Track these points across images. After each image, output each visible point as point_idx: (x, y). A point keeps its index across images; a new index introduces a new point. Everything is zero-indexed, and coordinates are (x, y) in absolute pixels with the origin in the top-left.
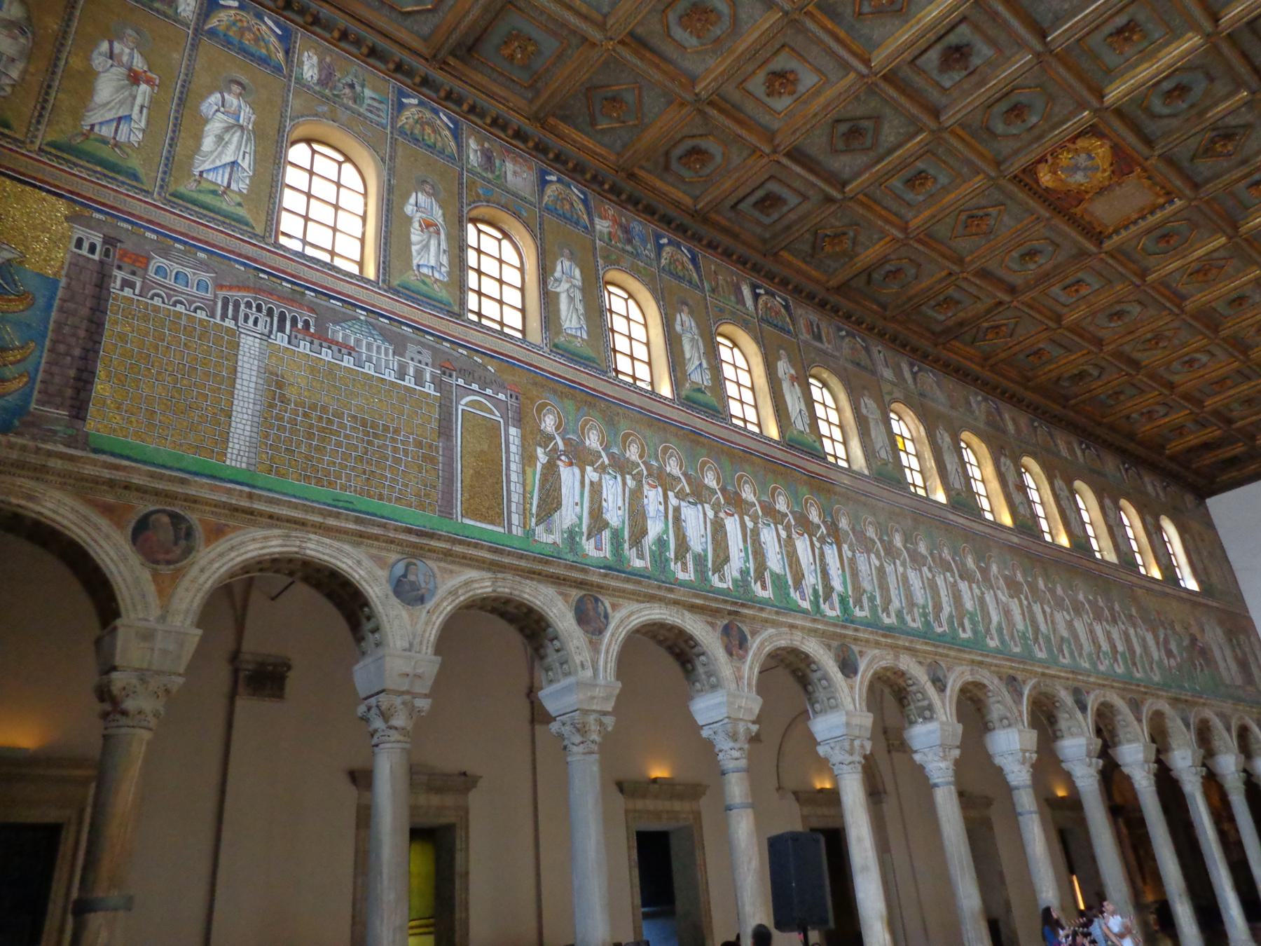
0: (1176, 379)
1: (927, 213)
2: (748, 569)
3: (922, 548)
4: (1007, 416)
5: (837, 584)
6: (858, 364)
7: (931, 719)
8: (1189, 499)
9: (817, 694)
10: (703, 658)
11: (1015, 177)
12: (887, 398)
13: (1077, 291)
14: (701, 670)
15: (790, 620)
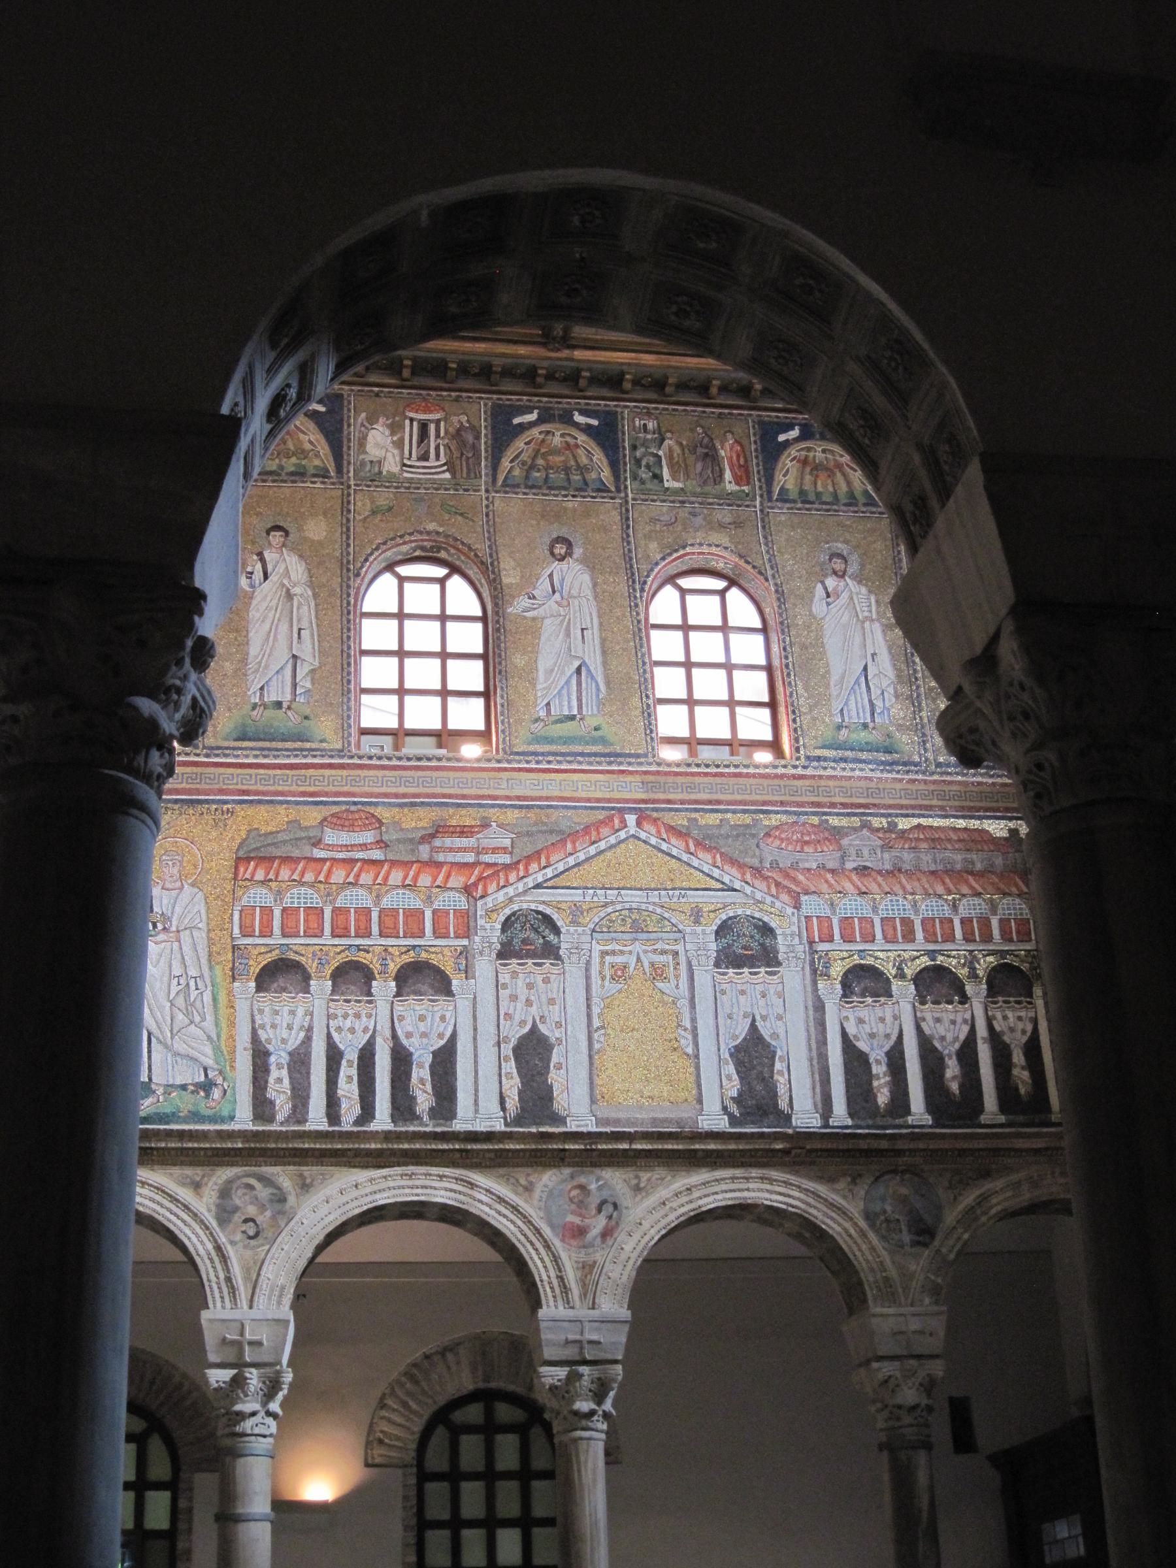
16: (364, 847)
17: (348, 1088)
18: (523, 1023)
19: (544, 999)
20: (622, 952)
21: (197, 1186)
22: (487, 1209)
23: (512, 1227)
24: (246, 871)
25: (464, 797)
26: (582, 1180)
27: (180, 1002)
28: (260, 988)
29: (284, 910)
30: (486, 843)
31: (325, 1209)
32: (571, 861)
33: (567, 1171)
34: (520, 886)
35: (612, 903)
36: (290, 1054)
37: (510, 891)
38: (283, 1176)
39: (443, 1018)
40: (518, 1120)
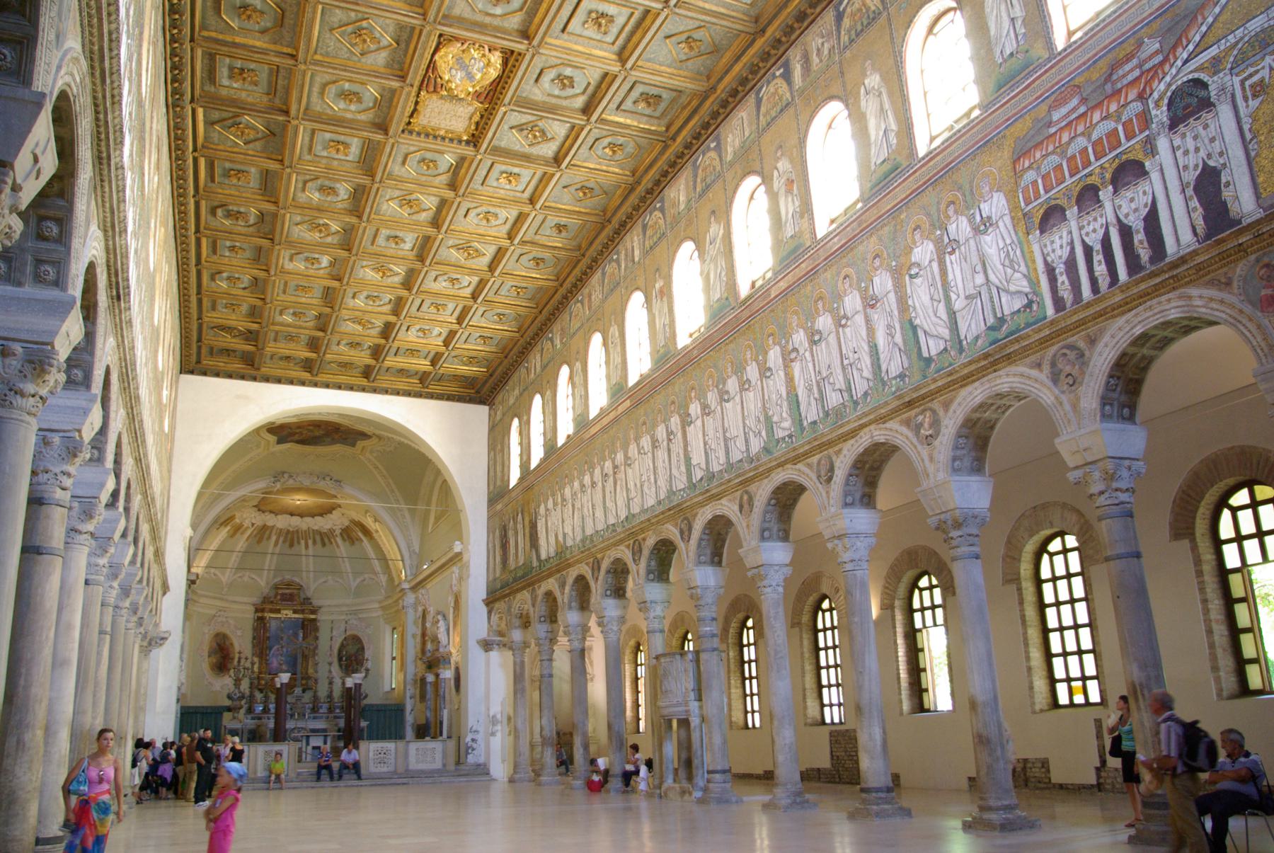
16: (1074, 110)
17: (1100, 269)
18: (1197, 166)
19: (1206, 141)
20: (1257, 72)
21: (1039, 366)
22: (1204, 310)
23: (1223, 315)
25: (1123, 34)
26: (1266, 260)
27: (1007, 263)
28: (1042, 232)
30: (1143, 56)
31: (1107, 350)
32: (1204, 28)
33: (1253, 257)
34: (1174, 71)
35: (1242, 38)
36: (1065, 263)
37: (1168, 79)
38: (1078, 340)
39: (1145, 193)
40: (1208, 236)
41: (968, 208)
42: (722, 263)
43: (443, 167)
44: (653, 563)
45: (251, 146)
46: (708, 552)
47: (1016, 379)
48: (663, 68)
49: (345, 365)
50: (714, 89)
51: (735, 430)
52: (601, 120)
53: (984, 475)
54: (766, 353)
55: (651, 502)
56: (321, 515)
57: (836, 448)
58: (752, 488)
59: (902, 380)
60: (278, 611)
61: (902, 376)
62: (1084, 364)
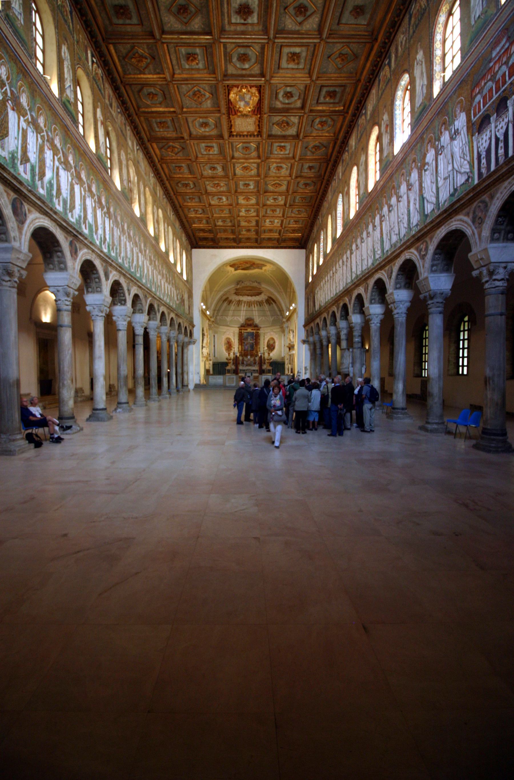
0: (213, 203)
1: (185, 76)
2: (81, 216)
3: (131, 234)
4: (158, 188)
5: (107, 237)
6: (122, 131)
7: (125, 304)
8: (190, 246)
9: (91, 284)
10: (59, 254)
11: (225, 86)
12: (129, 156)
13: (209, 150)
14: (56, 259)
15: (94, 248)
16: (504, 46)
17: (501, 151)
21: (468, 215)
24: (474, 94)
27: (462, 156)
28: (478, 134)
29: (484, 98)
38: (485, 197)
41: (450, 125)
42: (364, 175)
43: (253, 149)
44: (343, 313)
45: (178, 155)
46: (358, 308)
47: (458, 223)
48: (332, 75)
49: (248, 239)
50: (359, 80)
51: (365, 256)
52: (311, 111)
53: (451, 272)
54: (375, 218)
55: (341, 288)
56: (258, 295)
57: (394, 263)
58: (368, 282)
59: (417, 227)
60: (246, 330)
61: (417, 225)
62: (487, 211)
